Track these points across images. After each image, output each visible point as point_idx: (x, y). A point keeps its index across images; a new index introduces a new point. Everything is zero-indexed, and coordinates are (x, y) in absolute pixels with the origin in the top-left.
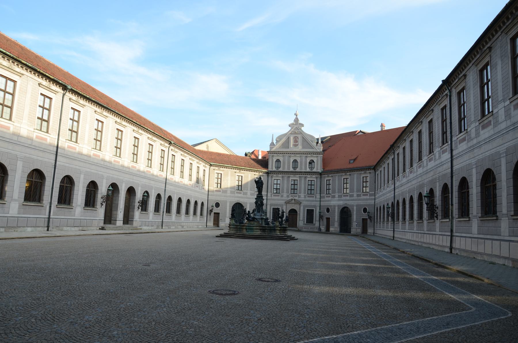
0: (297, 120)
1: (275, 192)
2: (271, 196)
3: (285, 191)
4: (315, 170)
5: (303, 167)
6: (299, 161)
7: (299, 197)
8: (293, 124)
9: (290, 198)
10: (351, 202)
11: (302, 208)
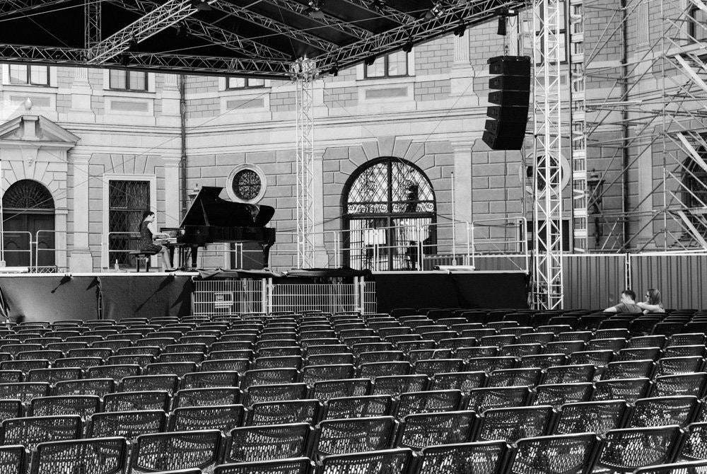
10: (428, 126)
11: (80, 175)
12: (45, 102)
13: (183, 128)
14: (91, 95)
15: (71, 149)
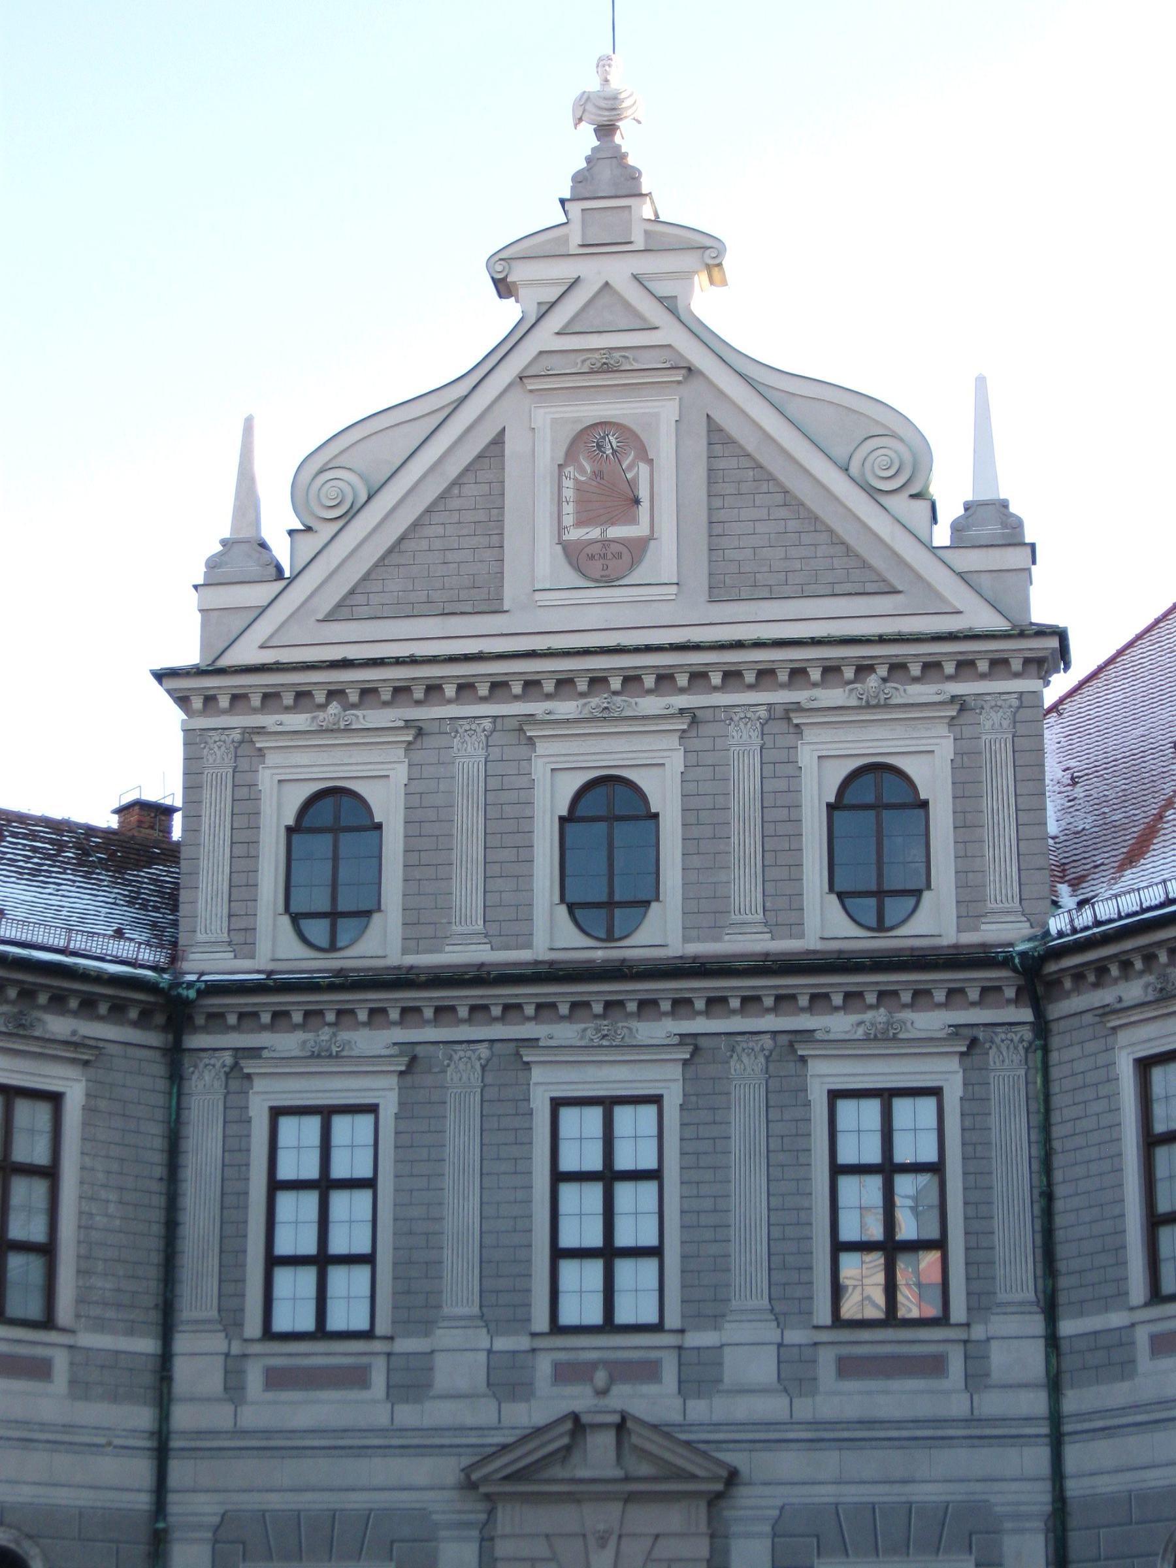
0: (607, 181)
1: (294, 1314)
2: (234, 1390)
3: (460, 1287)
4: (934, 922)
5: (745, 891)
6: (664, 792)
7: (700, 1374)
8: (537, 248)
9: (549, 1403)
12: (648, 1371)
13: (1056, 1418)
14: (780, 1345)
15: (719, 1496)
